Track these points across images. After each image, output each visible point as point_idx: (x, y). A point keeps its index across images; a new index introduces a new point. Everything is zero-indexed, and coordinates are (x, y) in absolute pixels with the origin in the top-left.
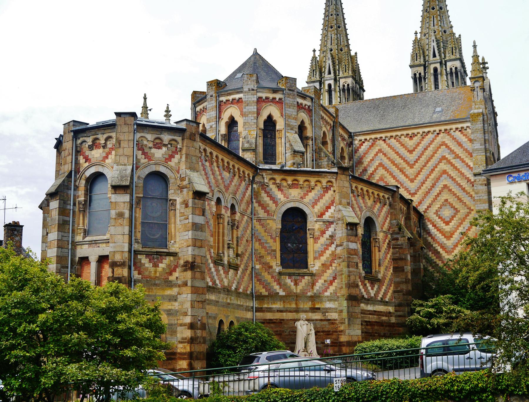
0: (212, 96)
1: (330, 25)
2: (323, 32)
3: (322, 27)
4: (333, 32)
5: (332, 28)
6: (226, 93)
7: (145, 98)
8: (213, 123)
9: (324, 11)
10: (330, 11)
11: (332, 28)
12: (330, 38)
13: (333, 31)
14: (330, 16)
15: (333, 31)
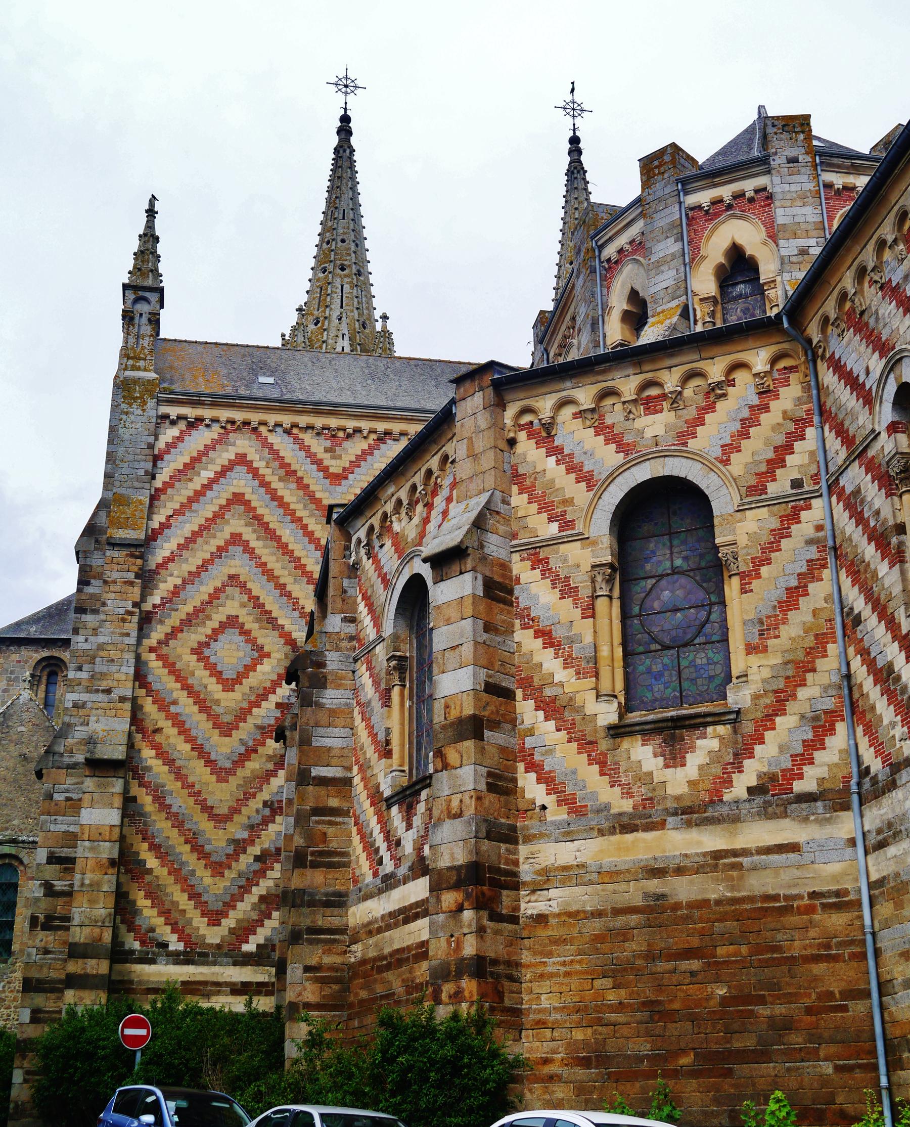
0: (793, 160)
1: (338, 262)
2: (315, 274)
3: (312, 263)
4: (346, 280)
5: (343, 269)
6: (848, 162)
7: (151, 213)
8: (813, 242)
9: (319, 229)
10: (340, 231)
11: (343, 269)
12: (339, 290)
13: (346, 276)
14: (340, 244)
15: (346, 276)
